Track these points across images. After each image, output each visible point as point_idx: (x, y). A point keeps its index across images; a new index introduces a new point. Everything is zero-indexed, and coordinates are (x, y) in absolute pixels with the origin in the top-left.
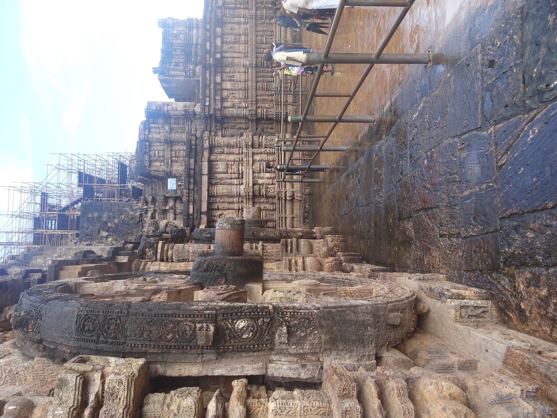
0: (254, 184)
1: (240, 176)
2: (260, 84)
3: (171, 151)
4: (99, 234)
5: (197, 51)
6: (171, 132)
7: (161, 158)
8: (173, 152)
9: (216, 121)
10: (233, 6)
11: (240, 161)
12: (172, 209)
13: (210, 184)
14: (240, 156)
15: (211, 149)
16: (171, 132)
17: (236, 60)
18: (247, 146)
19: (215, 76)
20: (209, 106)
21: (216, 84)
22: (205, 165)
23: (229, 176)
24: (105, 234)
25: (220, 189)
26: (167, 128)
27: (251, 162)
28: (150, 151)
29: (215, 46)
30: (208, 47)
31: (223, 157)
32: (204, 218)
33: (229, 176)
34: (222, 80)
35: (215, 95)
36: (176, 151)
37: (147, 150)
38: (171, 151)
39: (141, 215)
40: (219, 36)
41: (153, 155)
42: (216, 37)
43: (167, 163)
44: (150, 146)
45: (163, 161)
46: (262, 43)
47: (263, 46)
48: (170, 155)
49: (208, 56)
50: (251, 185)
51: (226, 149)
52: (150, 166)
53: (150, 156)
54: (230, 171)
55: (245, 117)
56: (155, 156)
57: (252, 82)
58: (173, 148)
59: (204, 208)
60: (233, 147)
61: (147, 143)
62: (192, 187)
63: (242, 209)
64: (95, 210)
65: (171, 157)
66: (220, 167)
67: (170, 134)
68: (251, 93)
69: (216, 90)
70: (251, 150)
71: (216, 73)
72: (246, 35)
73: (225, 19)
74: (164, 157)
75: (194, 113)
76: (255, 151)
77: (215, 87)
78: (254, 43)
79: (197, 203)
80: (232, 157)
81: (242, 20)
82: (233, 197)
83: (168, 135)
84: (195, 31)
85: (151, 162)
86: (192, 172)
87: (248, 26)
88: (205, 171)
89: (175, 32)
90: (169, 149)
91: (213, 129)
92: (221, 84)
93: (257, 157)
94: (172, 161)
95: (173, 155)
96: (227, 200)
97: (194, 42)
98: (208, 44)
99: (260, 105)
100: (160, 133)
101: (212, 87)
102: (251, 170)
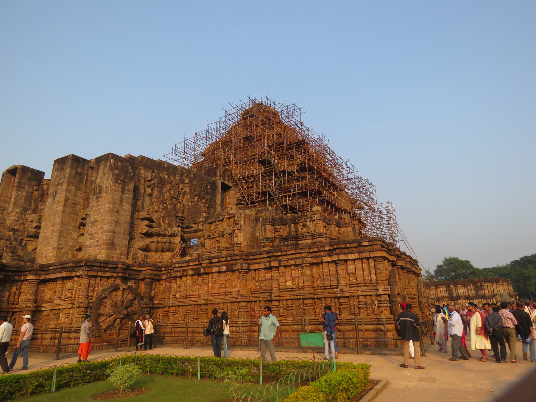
1: (65, 300)
3: (219, 237)
4: (196, 196)
8: (218, 238)
10: (257, 279)
19: (191, 269)
21: (187, 270)
24: (196, 200)
25: (59, 286)
29: (212, 267)
34: (192, 275)
35: (180, 271)
37: (217, 219)
38: (219, 237)
40: (219, 269)
42: (219, 266)
50: (55, 308)
53: (215, 222)
56: (216, 225)
57: (189, 301)
58: (221, 238)
59: (48, 277)
61: (221, 218)
62: (60, 267)
63: (50, 302)
65: (215, 238)
66: (69, 284)
69: (183, 271)
71: (194, 269)
74: (215, 232)
77: (185, 270)
79: (55, 271)
83: (225, 233)
89: (308, 223)
90: (219, 235)
94: (213, 238)
98: (216, 260)
102: (64, 307)
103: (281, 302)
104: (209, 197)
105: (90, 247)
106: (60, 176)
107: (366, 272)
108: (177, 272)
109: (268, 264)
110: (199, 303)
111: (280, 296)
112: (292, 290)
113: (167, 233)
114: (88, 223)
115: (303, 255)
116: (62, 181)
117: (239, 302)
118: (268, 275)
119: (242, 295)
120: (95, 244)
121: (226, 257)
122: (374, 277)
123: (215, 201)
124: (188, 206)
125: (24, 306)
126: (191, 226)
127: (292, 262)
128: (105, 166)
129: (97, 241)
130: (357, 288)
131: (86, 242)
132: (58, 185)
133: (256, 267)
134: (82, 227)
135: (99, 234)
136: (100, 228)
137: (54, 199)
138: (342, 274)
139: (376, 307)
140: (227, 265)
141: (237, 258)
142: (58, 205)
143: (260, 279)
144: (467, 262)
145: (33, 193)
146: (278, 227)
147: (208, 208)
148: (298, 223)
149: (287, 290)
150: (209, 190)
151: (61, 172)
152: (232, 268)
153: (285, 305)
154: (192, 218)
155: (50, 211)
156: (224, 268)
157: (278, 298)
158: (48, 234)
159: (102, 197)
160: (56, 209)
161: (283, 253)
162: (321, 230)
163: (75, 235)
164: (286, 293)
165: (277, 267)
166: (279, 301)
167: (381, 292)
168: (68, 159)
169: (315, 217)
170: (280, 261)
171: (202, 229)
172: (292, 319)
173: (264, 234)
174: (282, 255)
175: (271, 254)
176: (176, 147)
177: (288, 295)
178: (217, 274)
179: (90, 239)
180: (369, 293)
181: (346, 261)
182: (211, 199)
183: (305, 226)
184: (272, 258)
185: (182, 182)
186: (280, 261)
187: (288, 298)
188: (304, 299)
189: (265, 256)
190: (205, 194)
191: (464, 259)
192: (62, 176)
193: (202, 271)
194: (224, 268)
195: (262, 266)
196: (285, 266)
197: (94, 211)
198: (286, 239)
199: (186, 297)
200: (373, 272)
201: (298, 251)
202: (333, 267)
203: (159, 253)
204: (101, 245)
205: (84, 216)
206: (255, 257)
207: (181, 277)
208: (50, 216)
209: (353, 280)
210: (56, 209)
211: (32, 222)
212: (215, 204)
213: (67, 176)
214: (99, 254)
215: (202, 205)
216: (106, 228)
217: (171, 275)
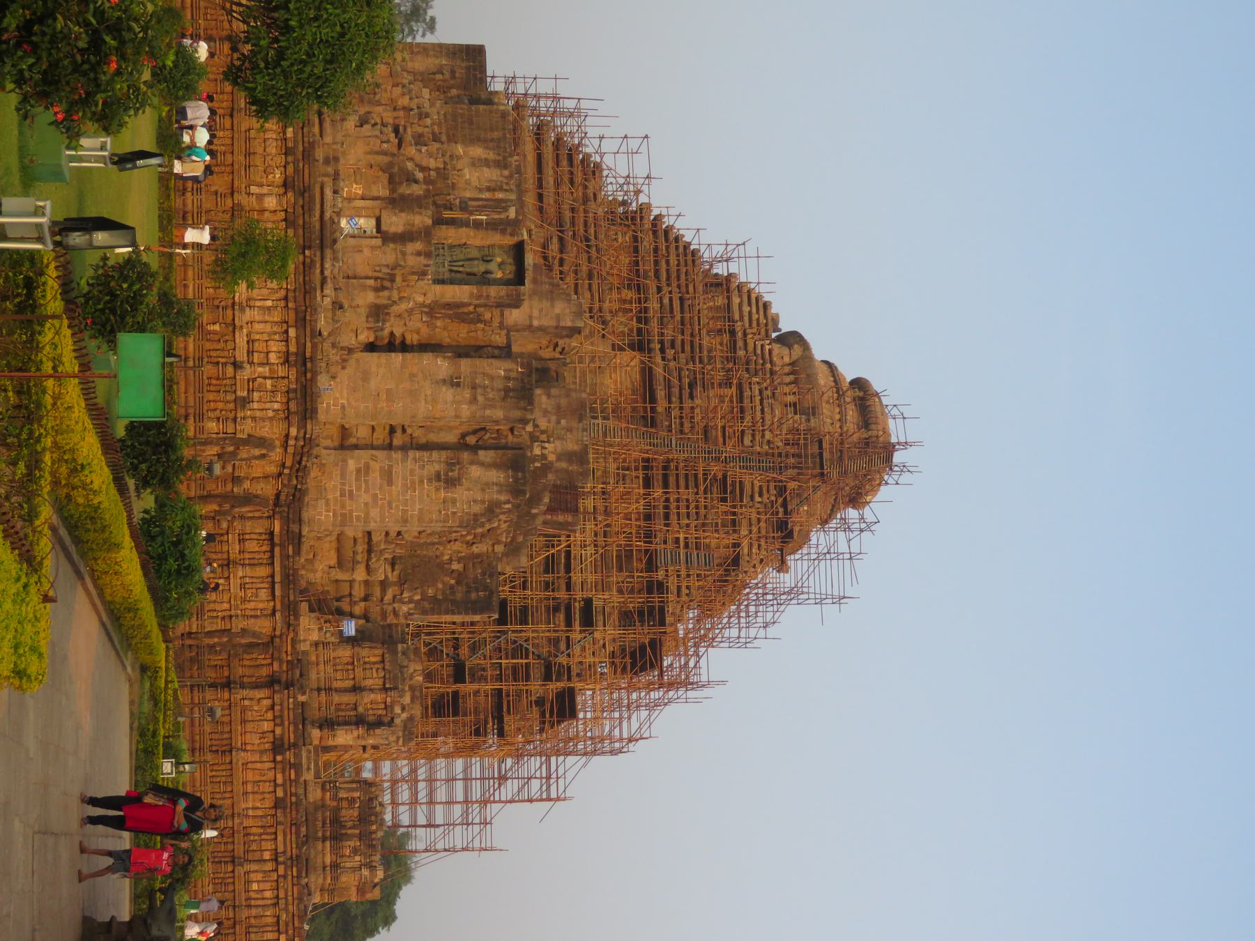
0: (228, 578)
1: (243, 586)
2: (227, 729)
3: (354, 679)
5: (323, 827)
6: (355, 704)
7: (368, 666)
8: (352, 676)
9: (279, 682)
10: (263, 837)
11: (244, 600)
12: (355, 602)
13: (272, 576)
14: (243, 607)
15: (273, 613)
16: (355, 704)
17: (256, 757)
19: (282, 735)
20: (289, 698)
22: (278, 593)
23: (254, 586)
25: (263, 571)
26: (360, 709)
28: (384, 677)
29: (284, 772)
30: (293, 772)
31: (261, 606)
32: (277, 540)
33: (254, 586)
34: (274, 732)
35: (281, 711)
38: (354, 679)
39: (402, 594)
42: (284, 785)
43: (359, 660)
44: (384, 684)
45: (365, 663)
46: (225, 783)
47: (223, 779)
49: (292, 760)
52: (383, 656)
53: (384, 669)
54: (254, 591)
55: (243, 686)
56: (377, 669)
57: (236, 730)
59: (277, 550)
60: (251, 616)
61: (387, 686)
64: (474, 602)
66: (264, 594)
68: (237, 715)
69: (281, 717)
70: (233, 612)
71: (282, 739)
73: (273, 812)
74: (364, 669)
75: (321, 728)
76: (227, 613)
78: (235, 783)
79: (285, 557)
80: (252, 605)
81: (251, 813)
82: (249, 565)
84: (328, 861)
85: (383, 661)
86: (292, 586)
87: (243, 806)
88: (277, 586)
89: (358, 858)
91: (285, 675)
92: (275, 725)
93: (226, 606)
96: (256, 562)
97: (328, 843)
98: (293, 777)
99: (227, 704)
101: (286, 723)
103: (231, 875)
104: (459, 596)
105: (343, 475)
106: (493, 390)
108: (281, 705)
109: (281, 859)
110: (234, 753)
111: (239, 876)
112: (247, 891)
113: (374, 560)
114: (390, 458)
115: (290, 907)
116: (480, 398)
117: (233, 816)
118: (267, 855)
119: (242, 823)
120: (347, 488)
121: (296, 795)
123: (447, 613)
124: (442, 554)
125: (235, 524)
126: (396, 567)
127: (282, 895)
128: (501, 485)
129: (351, 492)
131: (352, 458)
132: (474, 387)
133: (280, 838)
135: (365, 498)
136: (375, 496)
137: (444, 381)
140: (283, 799)
141: (294, 813)
142: (429, 399)
144: (389, 919)
145: (470, 304)
146: (357, 805)
147: (434, 597)
148: (360, 840)
149: (248, 882)
150: (473, 596)
151: (500, 390)
152: (280, 808)
154: (414, 567)
155: (420, 375)
156: (280, 793)
157: (236, 874)
158: (373, 383)
159: (438, 489)
160: (423, 395)
161: (295, 879)
162: (344, 879)
163: (373, 423)
165: (276, 870)
166: (233, 871)
168: (525, 409)
169: (365, 872)
170: (285, 877)
171: (386, 598)
173: (344, 789)
174: (293, 877)
175: (295, 863)
176: (738, 245)
177: (239, 886)
178: (273, 778)
179: (358, 471)
182: (453, 602)
183: (355, 851)
184: (289, 863)
185: (499, 542)
186: (285, 877)
188: (234, 907)
189: (294, 851)
190: (468, 585)
191: (400, 907)
192: (491, 396)
193: (279, 758)
194: (280, 793)
195: (281, 849)
196: (277, 881)
197: (412, 471)
198: (336, 821)
201: (296, 902)
203: (334, 545)
204: (343, 506)
205: (409, 431)
206: (294, 836)
207: (272, 708)
208: (412, 376)
210: (423, 395)
212: (439, 614)
213: (488, 412)
214: (327, 504)
215: (440, 586)
216: (374, 513)
217: (279, 692)
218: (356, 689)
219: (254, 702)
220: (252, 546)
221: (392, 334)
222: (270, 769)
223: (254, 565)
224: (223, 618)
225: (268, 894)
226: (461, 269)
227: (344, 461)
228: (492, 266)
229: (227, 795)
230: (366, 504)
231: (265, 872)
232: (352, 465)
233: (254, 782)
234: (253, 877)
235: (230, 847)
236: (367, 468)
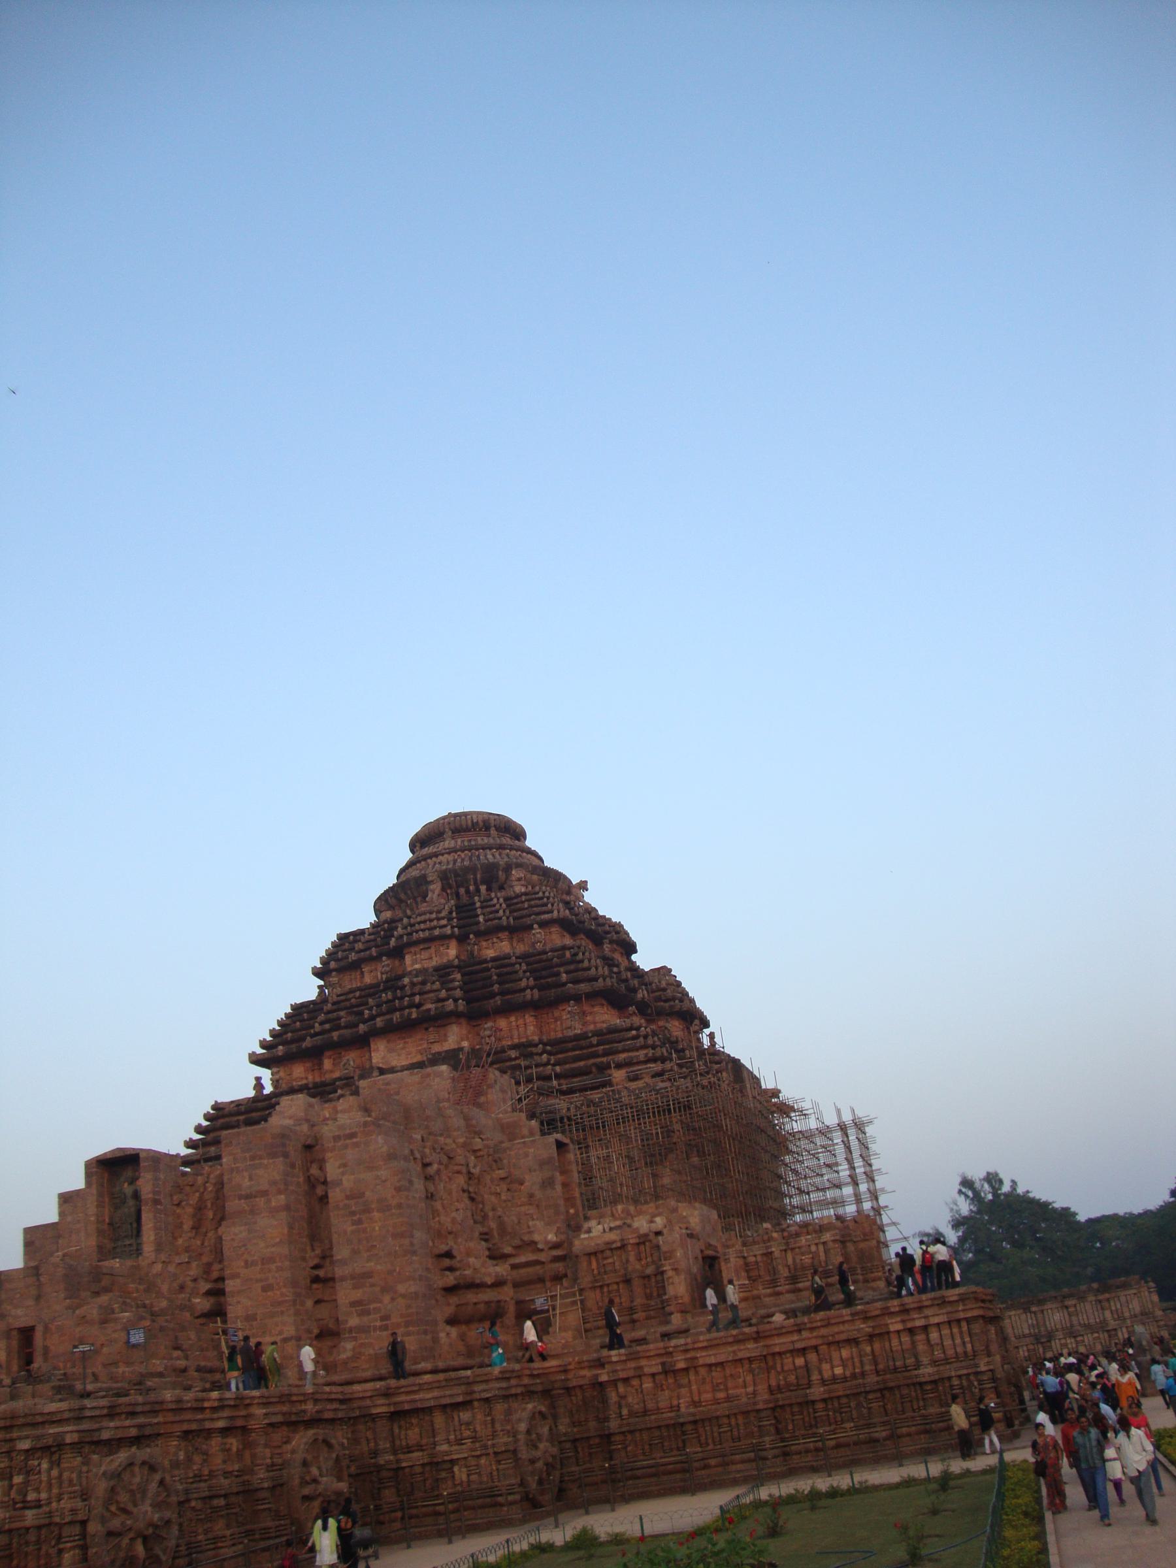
1: (459, 1442)
3: (617, 1283)
8: (615, 1287)
10: (779, 1369)
11: (475, 1439)
16: (644, 1278)
18: (493, 1445)
27: (473, 1453)
31: (479, 1416)
36: (618, 1290)
38: (617, 1283)
41: (605, 1255)
48: (609, 1282)
50: (446, 1458)
51: (489, 1418)
56: (606, 1258)
58: (621, 1286)
60: (493, 1427)
63: (422, 1450)
65: (608, 1285)
66: (465, 1416)
67: (638, 1277)
72: (728, 1399)
74: (605, 1272)
81: (750, 1389)
90: (618, 1280)
94: (601, 1287)
95: (610, 1288)
100: (640, 1260)
102: (466, 1455)
107: (958, 1341)
112: (845, 1379)
118: (800, 1361)
120: (378, 1324)
122: (969, 1346)
125: (382, 1462)
129: (383, 1318)
130: (948, 1366)
131: (347, 1321)
133: (777, 1349)
134: (315, 1286)
136: (385, 1289)
138: (921, 1347)
139: (977, 1390)
143: (786, 1368)
149: (834, 1379)
153: (836, 1404)
157: (826, 1396)
163: (309, 1303)
164: (836, 1386)
167: (983, 1368)
172: (852, 1425)
177: (839, 1390)
180: (965, 1372)
181: (925, 1328)
187: (841, 1393)
199: (645, 1412)
200: (967, 1339)
202: (906, 1339)
205: (316, 1261)
209: (938, 1354)
211: (195, 1280)
218: (628, 1281)
219: (623, 1402)
220: (413, 1435)
221: (209, 1293)
222: (697, 1373)
223: (433, 1431)
224: (499, 1462)
225: (845, 1353)
226: (135, 1225)
227: (351, 1330)
228: (128, 1189)
229: (733, 1421)
230: (393, 1299)
231: (820, 1361)
232: (354, 1321)
233: (714, 1391)
234: (827, 1374)
235: (796, 1409)
236: (353, 1304)
